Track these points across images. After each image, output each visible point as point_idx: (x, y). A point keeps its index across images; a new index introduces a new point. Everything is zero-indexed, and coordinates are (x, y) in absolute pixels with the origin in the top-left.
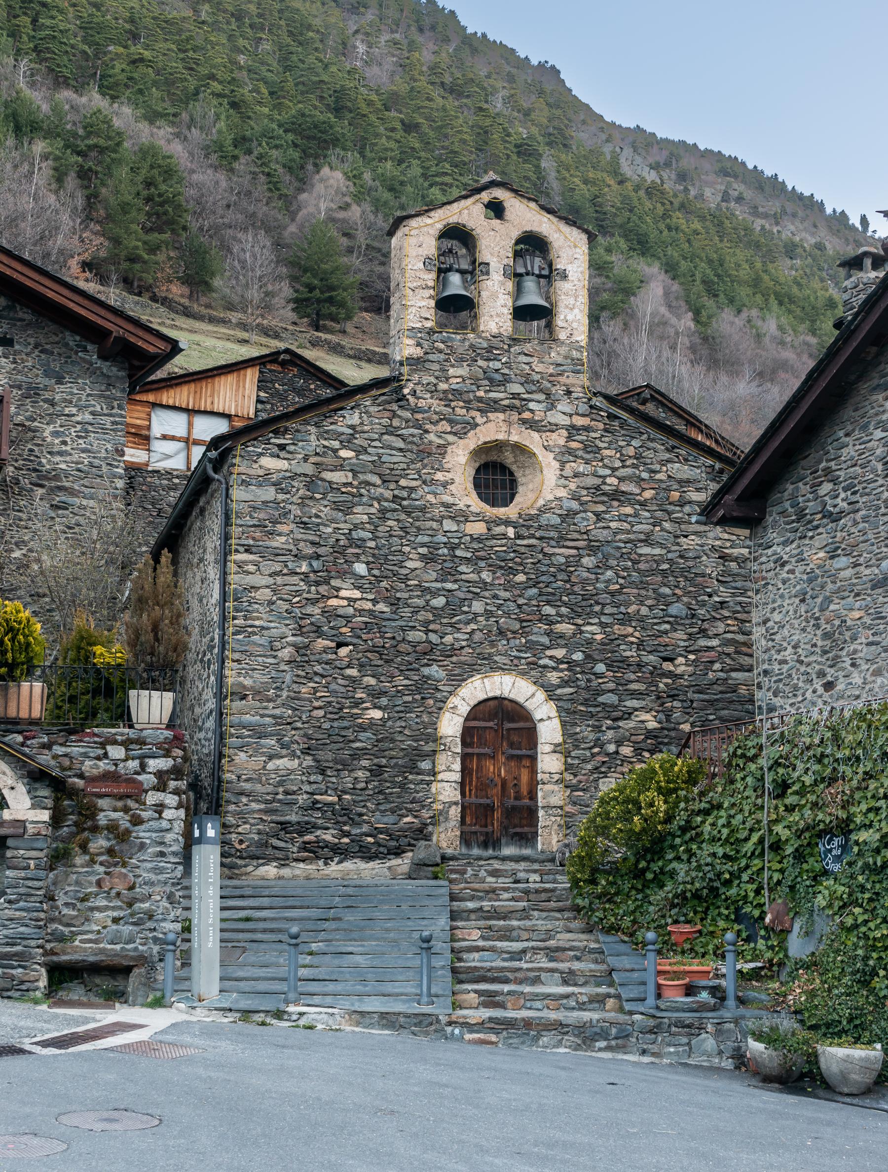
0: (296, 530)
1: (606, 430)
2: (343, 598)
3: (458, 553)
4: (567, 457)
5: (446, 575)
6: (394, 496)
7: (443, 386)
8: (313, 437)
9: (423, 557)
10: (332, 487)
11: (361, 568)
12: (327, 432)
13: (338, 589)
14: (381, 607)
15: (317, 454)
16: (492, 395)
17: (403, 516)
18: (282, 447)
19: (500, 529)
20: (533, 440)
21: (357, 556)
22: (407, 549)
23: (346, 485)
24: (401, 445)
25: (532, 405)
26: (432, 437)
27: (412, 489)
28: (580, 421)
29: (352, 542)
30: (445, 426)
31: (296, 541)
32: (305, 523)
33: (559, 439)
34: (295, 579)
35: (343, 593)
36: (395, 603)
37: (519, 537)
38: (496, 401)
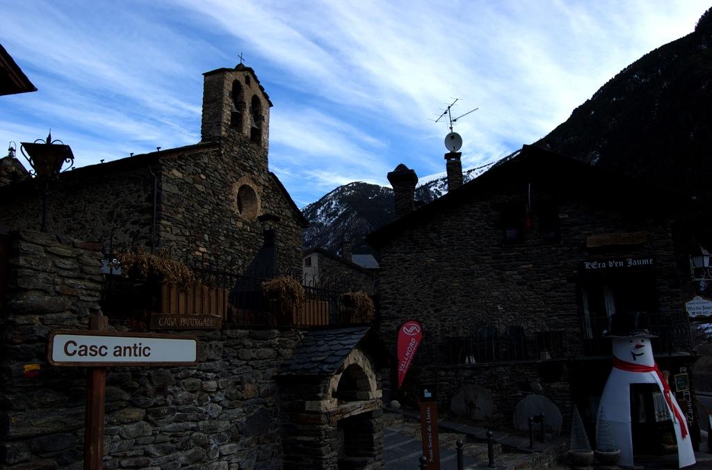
0: (185, 212)
1: (272, 190)
2: (200, 252)
3: (236, 236)
4: (263, 199)
5: (232, 245)
6: (217, 203)
7: (232, 154)
8: (192, 164)
9: (226, 236)
10: (199, 193)
11: (206, 237)
12: (198, 163)
13: (199, 246)
14: (212, 258)
15: (193, 174)
16: (245, 164)
17: (219, 214)
18: (180, 166)
19: (246, 226)
20: (255, 188)
21: (205, 230)
22: (220, 230)
23: (203, 192)
24: (219, 178)
25: (255, 172)
26: (229, 176)
27: (222, 201)
28: (267, 184)
29: (205, 224)
30: (232, 173)
31: (184, 218)
32: (188, 209)
33: (261, 188)
34: (184, 239)
35: (201, 249)
36: (217, 257)
37: (251, 232)
38: (246, 166)
